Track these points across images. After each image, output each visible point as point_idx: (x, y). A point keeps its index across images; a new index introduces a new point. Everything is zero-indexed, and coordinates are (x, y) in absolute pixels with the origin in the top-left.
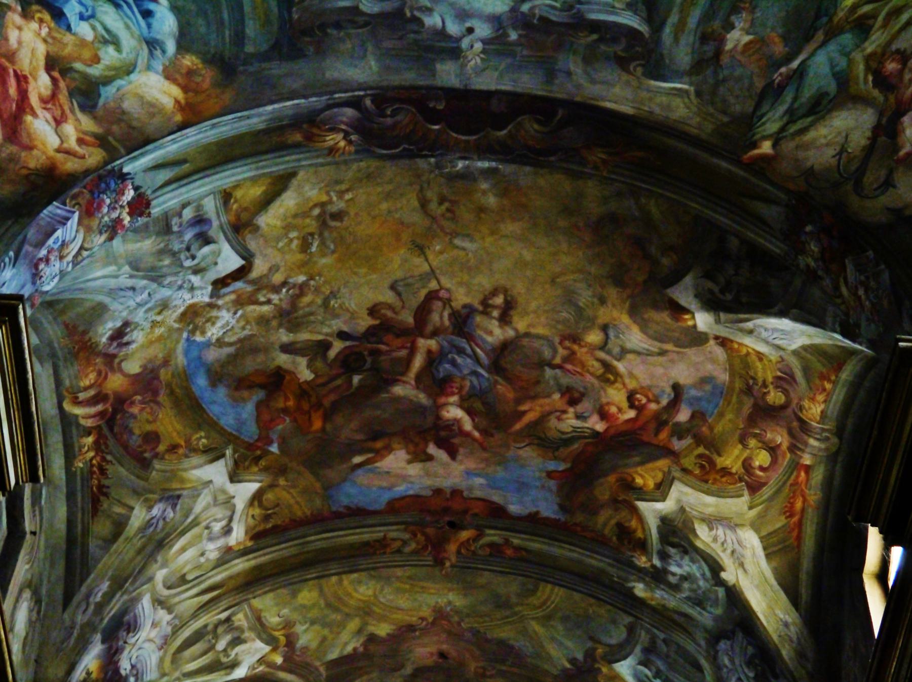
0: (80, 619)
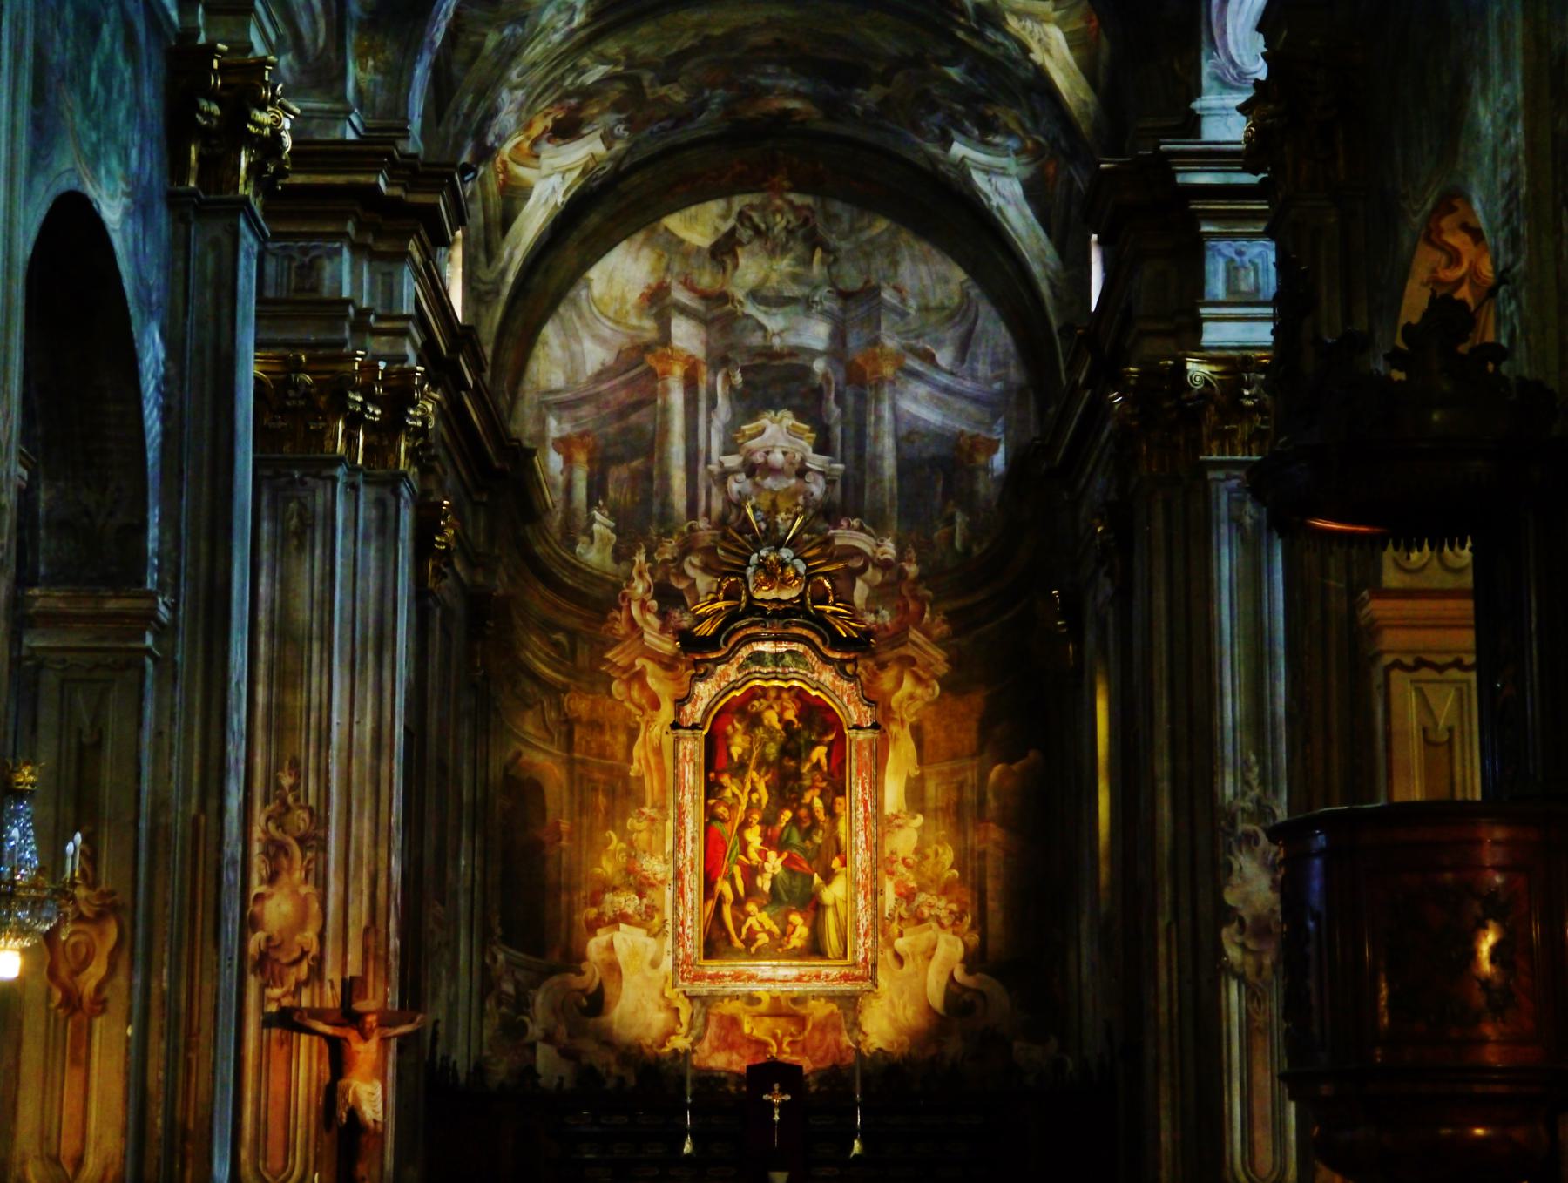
0: (453, 130)
